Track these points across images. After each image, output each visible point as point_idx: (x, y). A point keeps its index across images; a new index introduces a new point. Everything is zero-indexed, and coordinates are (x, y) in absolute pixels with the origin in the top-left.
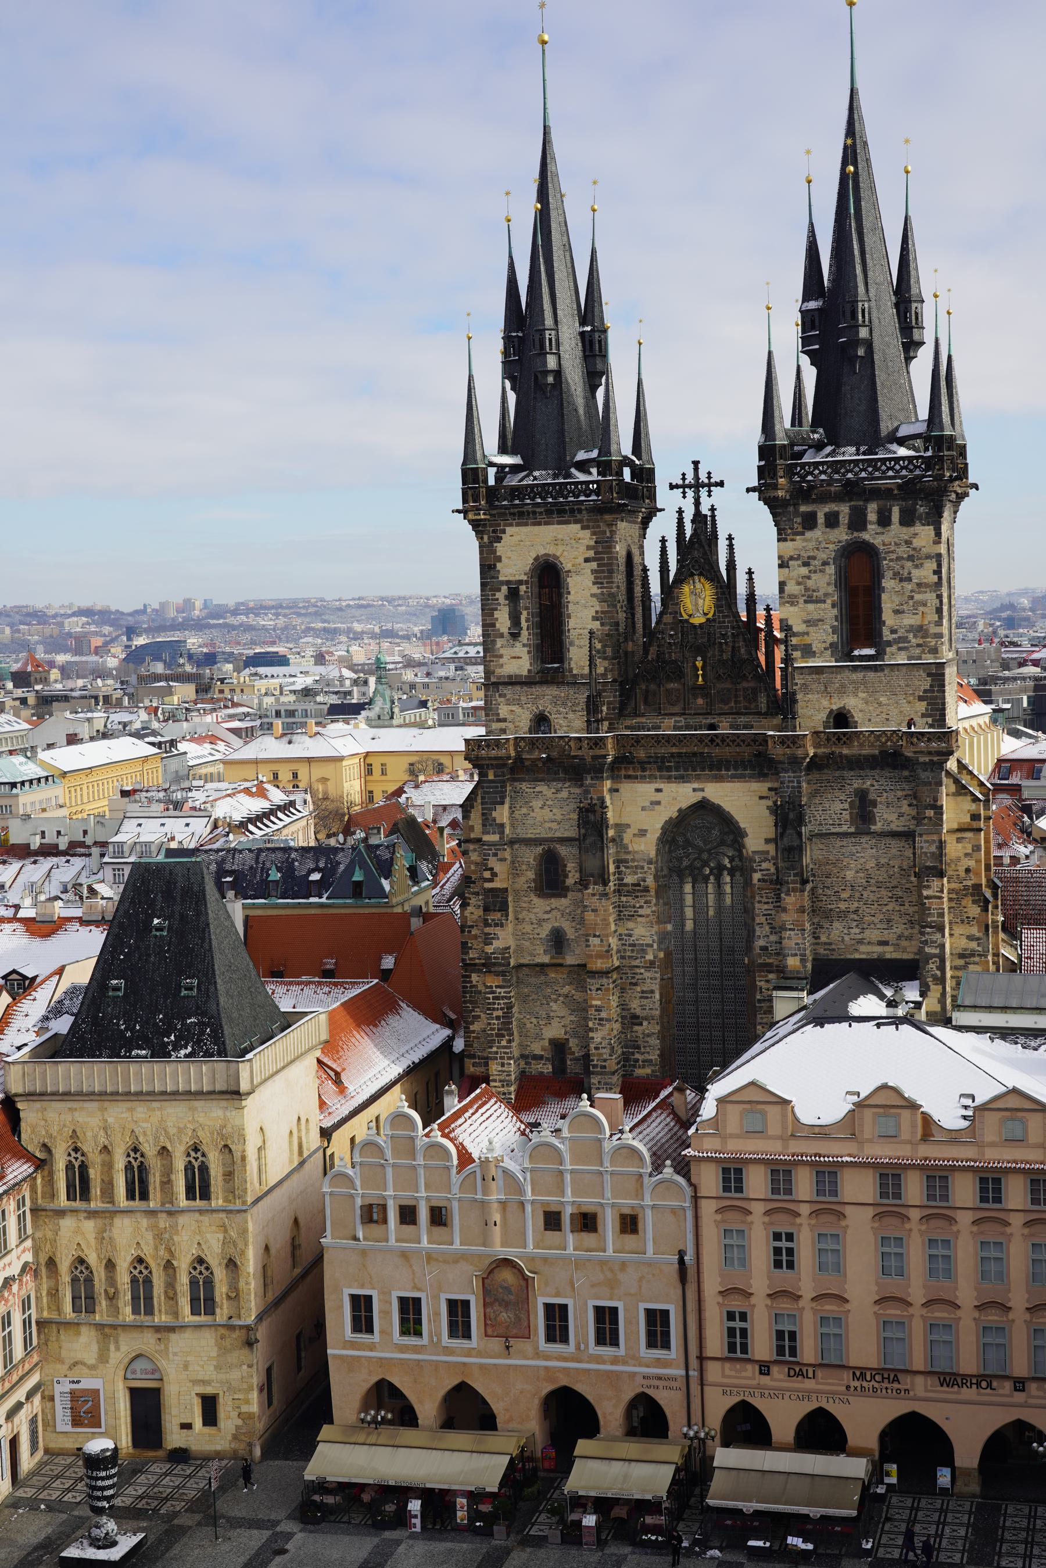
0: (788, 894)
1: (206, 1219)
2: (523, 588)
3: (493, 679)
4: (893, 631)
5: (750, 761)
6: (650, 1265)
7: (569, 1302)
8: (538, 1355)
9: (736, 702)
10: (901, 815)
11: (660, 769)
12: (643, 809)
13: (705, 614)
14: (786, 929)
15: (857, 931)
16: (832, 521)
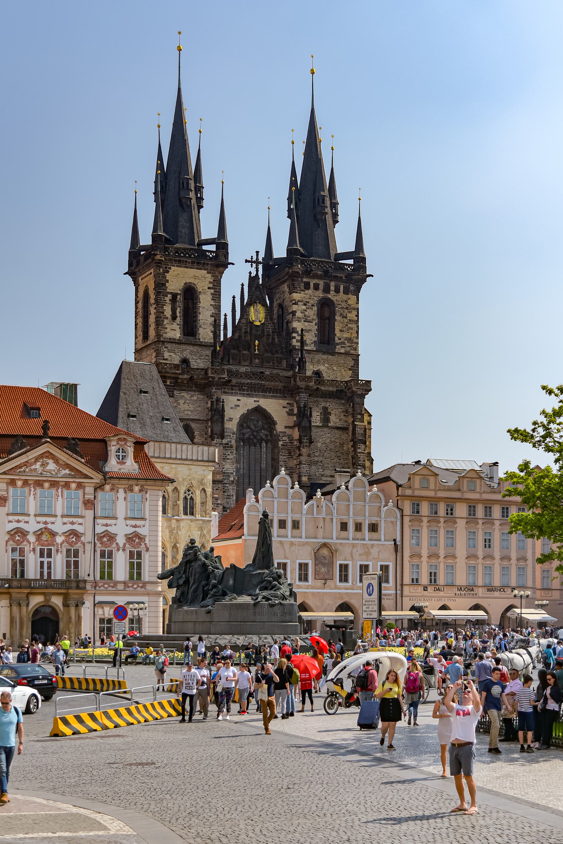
0: (303, 448)
1: (193, 524)
2: (179, 297)
3: (162, 339)
4: (340, 339)
5: (280, 390)
6: (383, 545)
7: (350, 563)
8: (336, 588)
9: (273, 363)
10: (341, 420)
11: (240, 390)
12: (231, 408)
13: (260, 321)
14: (302, 464)
15: (321, 470)
16: (316, 287)
